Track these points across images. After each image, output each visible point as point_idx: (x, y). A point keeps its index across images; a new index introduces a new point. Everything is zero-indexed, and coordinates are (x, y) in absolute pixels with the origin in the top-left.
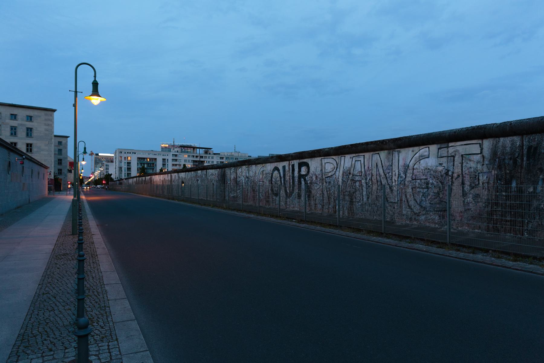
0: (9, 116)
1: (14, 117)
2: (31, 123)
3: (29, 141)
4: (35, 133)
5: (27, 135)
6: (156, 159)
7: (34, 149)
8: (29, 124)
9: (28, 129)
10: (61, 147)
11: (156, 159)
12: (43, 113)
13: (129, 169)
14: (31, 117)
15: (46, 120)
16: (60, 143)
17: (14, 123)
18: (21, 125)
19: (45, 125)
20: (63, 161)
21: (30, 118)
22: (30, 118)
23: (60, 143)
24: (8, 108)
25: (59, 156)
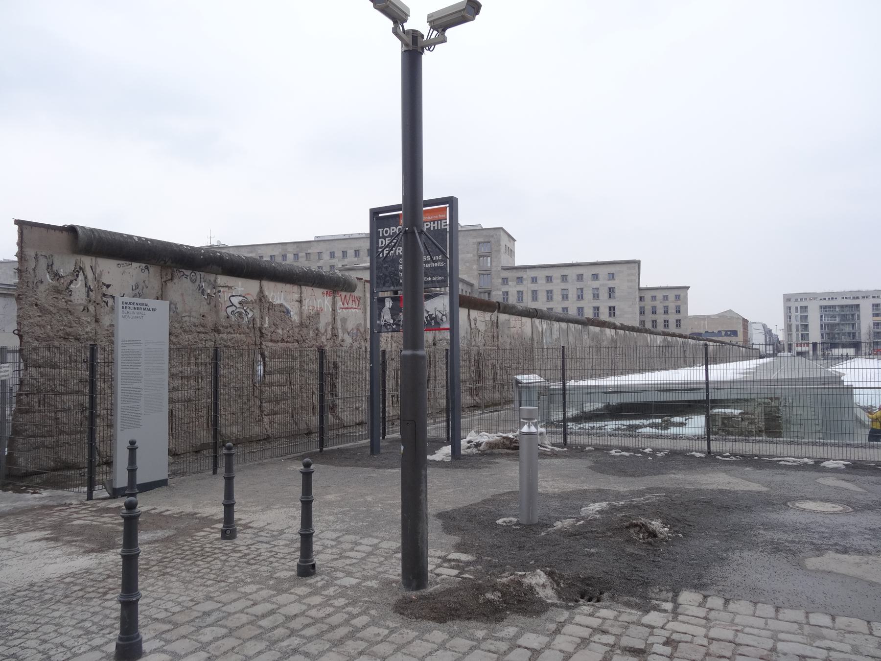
0: (591, 276)
1: (595, 277)
2: (613, 282)
3: (612, 304)
4: (617, 293)
5: (610, 296)
6: (858, 306)
7: (617, 313)
8: (611, 284)
9: (610, 289)
10: (679, 303)
11: (858, 306)
12: (624, 268)
13: (806, 327)
14: (613, 274)
16: (678, 297)
17: (596, 284)
19: (628, 281)
20: (682, 322)
21: (612, 276)
22: (612, 276)
23: (678, 297)
24: (589, 267)
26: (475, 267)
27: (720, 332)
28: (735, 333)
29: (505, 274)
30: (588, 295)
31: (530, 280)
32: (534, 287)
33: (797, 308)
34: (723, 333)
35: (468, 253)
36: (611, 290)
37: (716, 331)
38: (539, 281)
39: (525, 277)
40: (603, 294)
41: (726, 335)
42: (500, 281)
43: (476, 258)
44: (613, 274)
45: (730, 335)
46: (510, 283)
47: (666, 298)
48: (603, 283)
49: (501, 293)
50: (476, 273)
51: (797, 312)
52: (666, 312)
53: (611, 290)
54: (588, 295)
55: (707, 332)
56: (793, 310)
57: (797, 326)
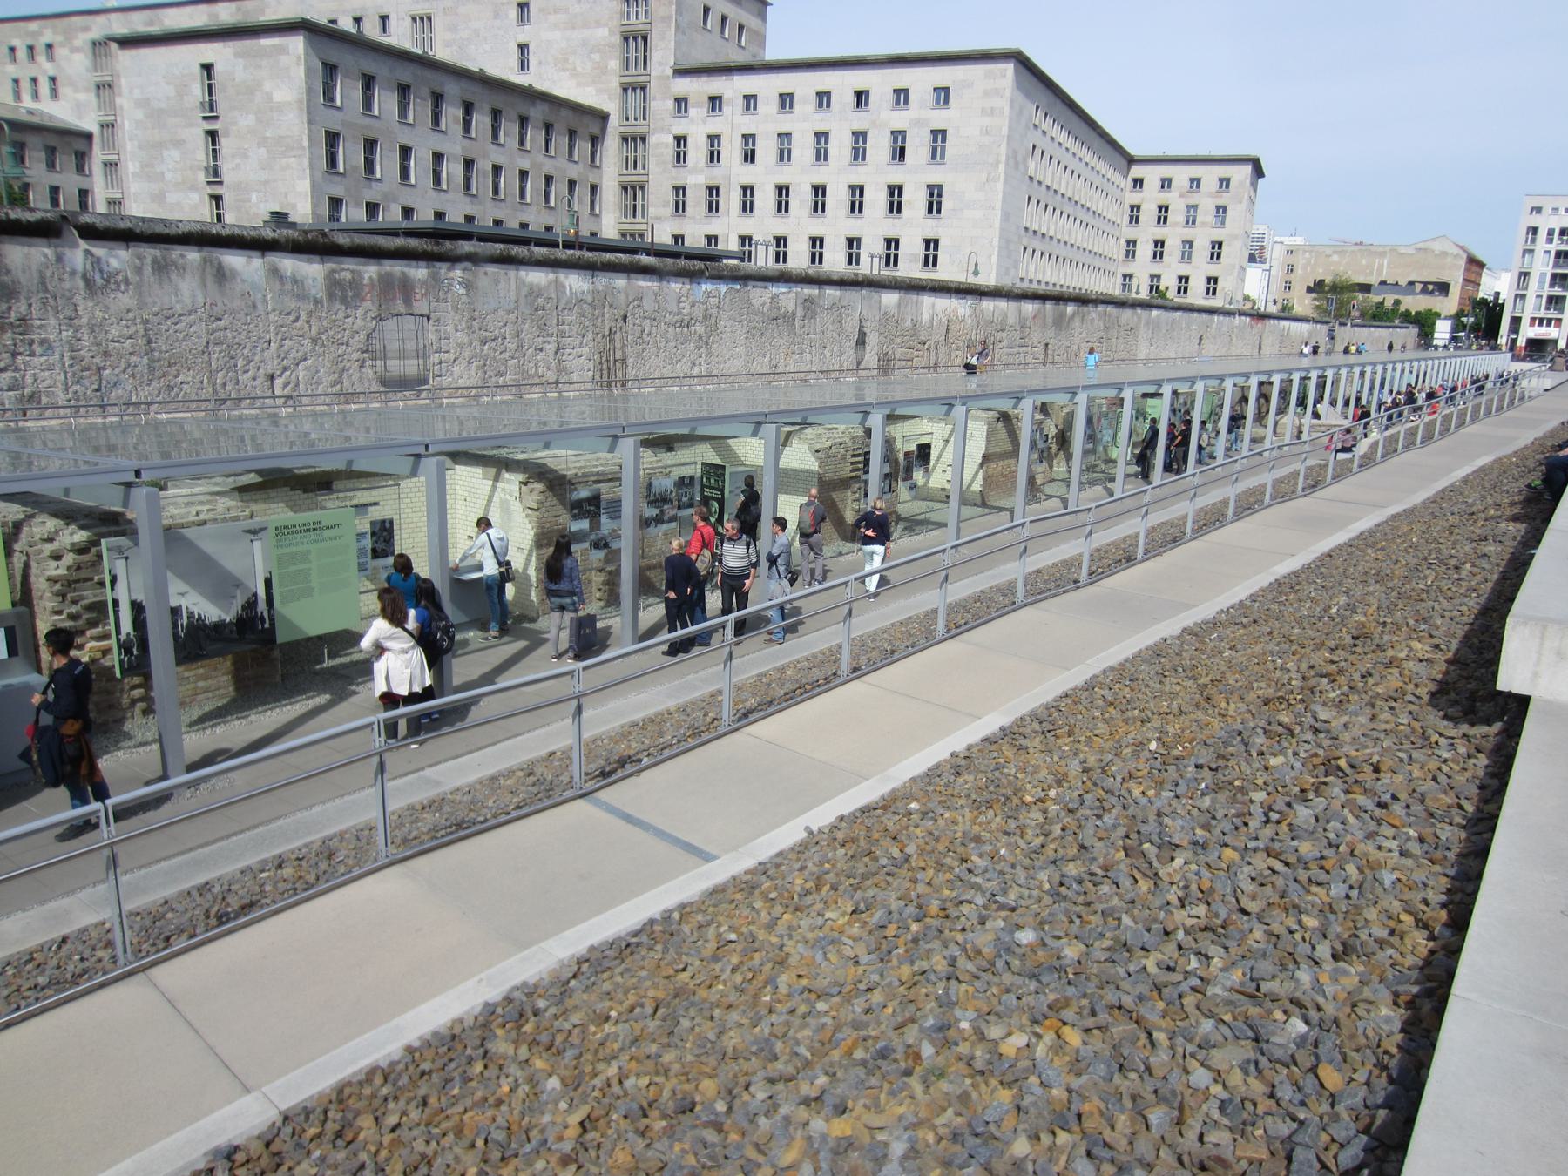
5: (934, 156)
8: (939, 119)
14: (946, 90)
15: (986, 94)
17: (899, 119)
18: (918, 122)
19: (984, 112)
21: (942, 94)
22: (942, 94)
25: (1187, 230)
26: (614, 64)
27: (1411, 283)
28: (1443, 288)
29: (685, 86)
30: (879, 147)
31: (741, 102)
32: (748, 124)
33: (1551, 233)
34: (1419, 287)
35: (598, 24)
36: (939, 135)
37: (1403, 283)
38: (762, 107)
39: (727, 95)
40: (918, 147)
41: (1425, 291)
42: (670, 104)
43: (618, 39)
44: (946, 90)
45: (1432, 293)
46: (692, 111)
47: (1196, 182)
48: (918, 118)
49: (671, 140)
50: (615, 84)
51: (1550, 241)
52: (1191, 221)
53: (939, 135)
54: (879, 147)
55: (1383, 283)
56: (1542, 235)
57: (1543, 275)
